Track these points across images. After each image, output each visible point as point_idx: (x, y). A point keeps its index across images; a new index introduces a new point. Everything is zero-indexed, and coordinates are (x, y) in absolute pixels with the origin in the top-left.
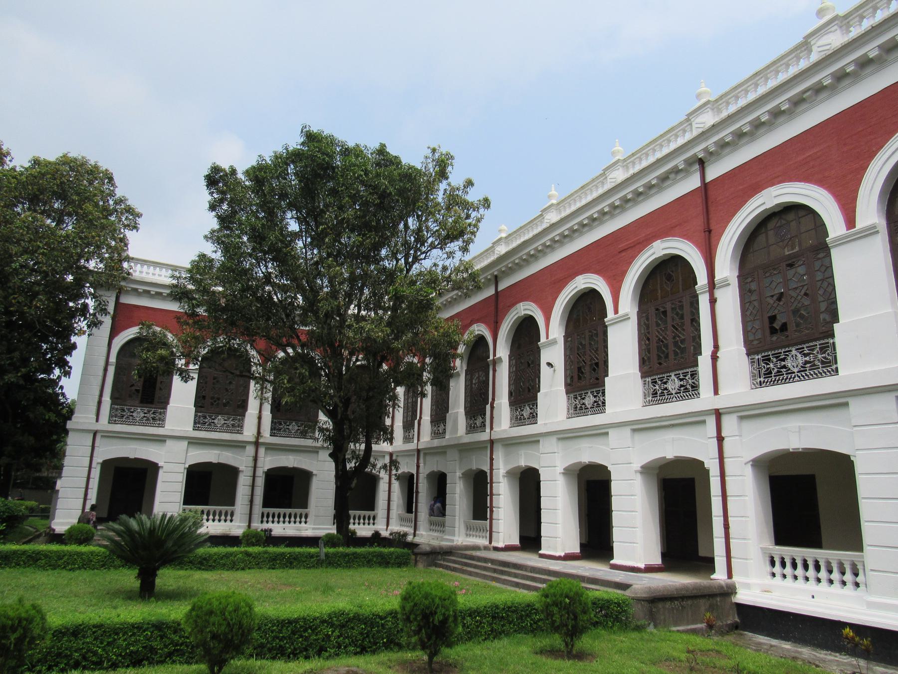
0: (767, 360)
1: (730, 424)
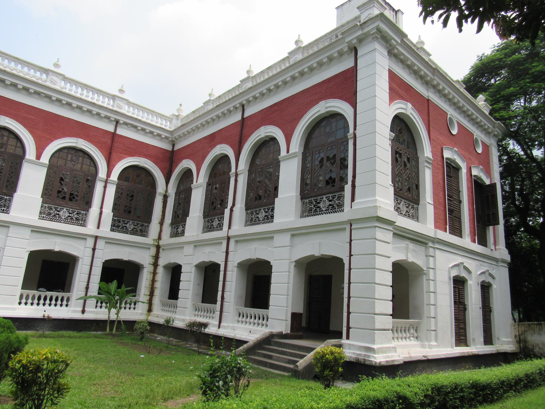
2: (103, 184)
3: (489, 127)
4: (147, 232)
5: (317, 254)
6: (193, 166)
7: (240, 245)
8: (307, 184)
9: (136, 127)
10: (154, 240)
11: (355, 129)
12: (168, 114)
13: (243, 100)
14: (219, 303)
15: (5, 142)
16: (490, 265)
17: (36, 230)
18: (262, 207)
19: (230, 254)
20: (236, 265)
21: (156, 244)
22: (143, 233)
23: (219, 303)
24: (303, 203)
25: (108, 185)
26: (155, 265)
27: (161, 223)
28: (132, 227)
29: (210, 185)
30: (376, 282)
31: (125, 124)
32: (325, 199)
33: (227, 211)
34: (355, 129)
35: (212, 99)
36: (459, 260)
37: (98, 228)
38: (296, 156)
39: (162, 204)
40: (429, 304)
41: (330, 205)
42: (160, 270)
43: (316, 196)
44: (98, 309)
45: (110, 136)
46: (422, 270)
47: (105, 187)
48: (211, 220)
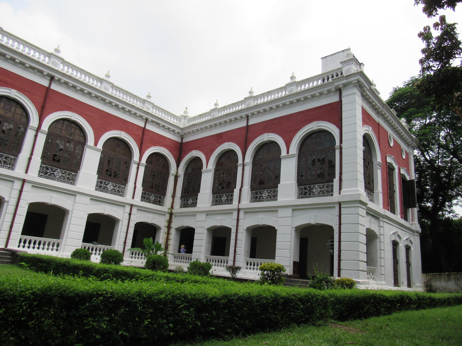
0: (47, 169)
1: (27, 187)
2: (136, 166)
3: (410, 141)
4: (163, 203)
5: (313, 222)
6: (202, 156)
7: (248, 215)
8: (302, 176)
9: (158, 124)
10: (169, 209)
11: (341, 142)
12: (178, 115)
13: (249, 113)
15: (73, 132)
16: (410, 235)
17: (94, 199)
18: (265, 189)
19: (240, 221)
20: (245, 229)
21: (170, 211)
22: (160, 202)
24: (299, 189)
25: (140, 167)
26: (169, 227)
27: (173, 196)
28: (154, 198)
29: (217, 170)
30: (360, 241)
31: (152, 121)
32: (316, 186)
33: (236, 191)
34: (341, 142)
35: (219, 107)
36: (395, 230)
37: (133, 198)
38: (295, 156)
39: (174, 182)
40: (381, 258)
41: (321, 191)
42: (173, 231)
43: (310, 184)
44: (133, 259)
45: (141, 131)
46: (376, 235)
47: (138, 168)
48: (220, 196)
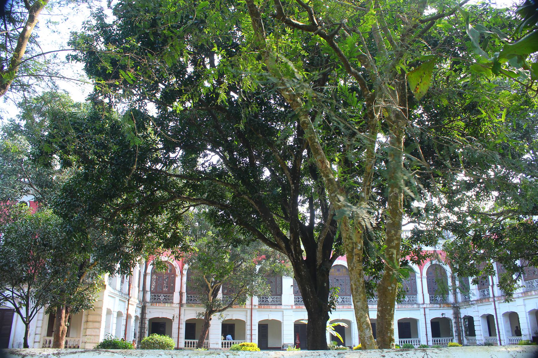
14: (498, 335)
23: (498, 335)
33: (490, 288)
47: (422, 281)
